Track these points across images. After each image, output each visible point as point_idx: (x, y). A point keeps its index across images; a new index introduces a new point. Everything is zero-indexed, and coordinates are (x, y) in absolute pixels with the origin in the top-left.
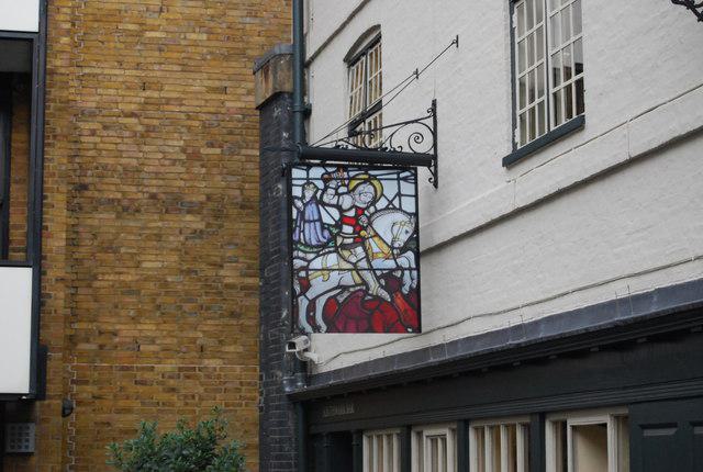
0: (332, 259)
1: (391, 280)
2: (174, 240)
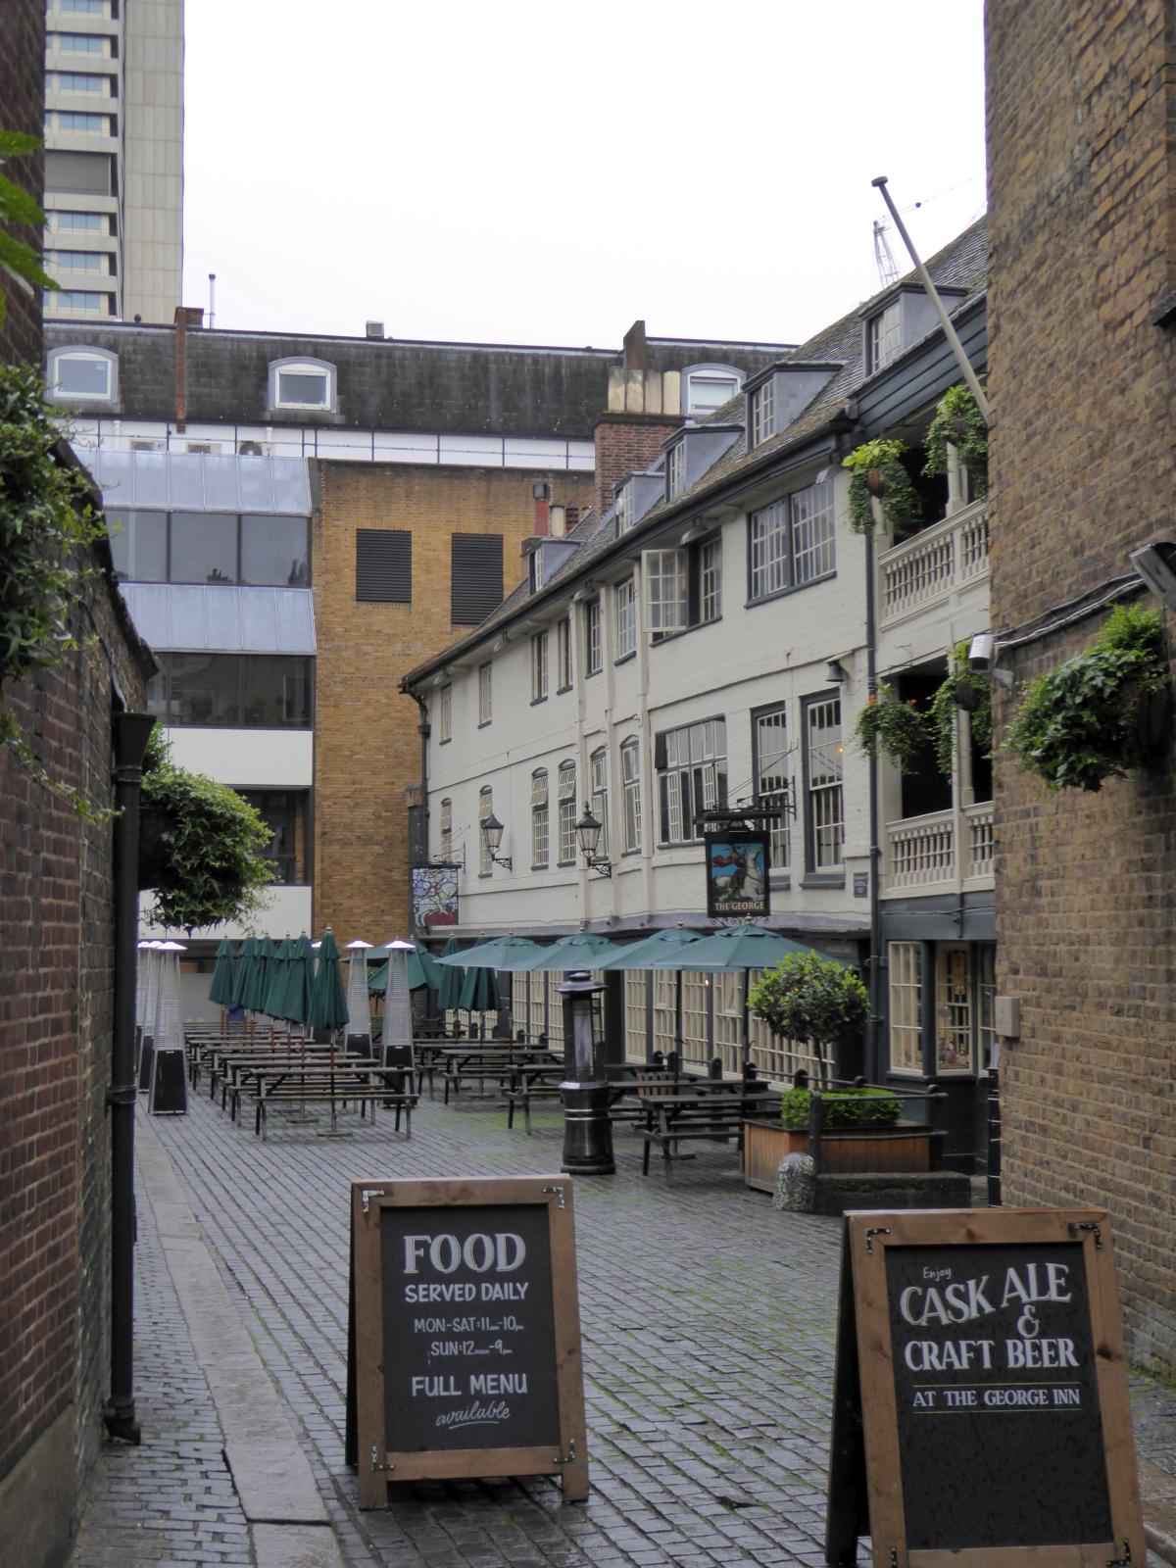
0: (427, 901)
1: (448, 907)
2: (369, 859)
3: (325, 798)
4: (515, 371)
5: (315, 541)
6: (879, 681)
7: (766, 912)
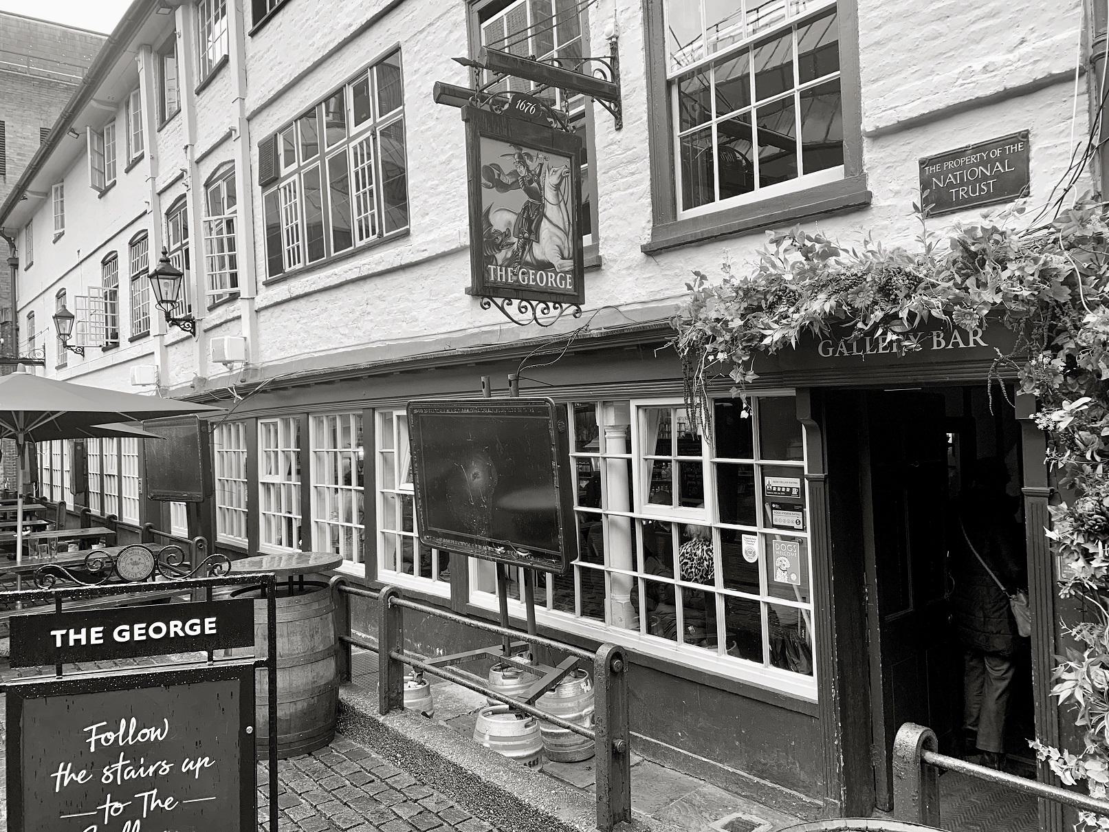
7: (577, 298)
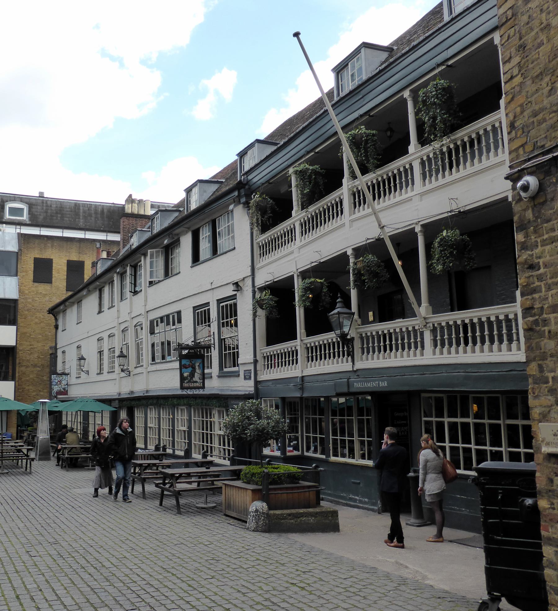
0: (57, 386)
1: (64, 389)
2: (35, 372)
3: (20, 350)
4: (89, 210)
5: (19, 261)
6: (256, 290)
7: (203, 387)
